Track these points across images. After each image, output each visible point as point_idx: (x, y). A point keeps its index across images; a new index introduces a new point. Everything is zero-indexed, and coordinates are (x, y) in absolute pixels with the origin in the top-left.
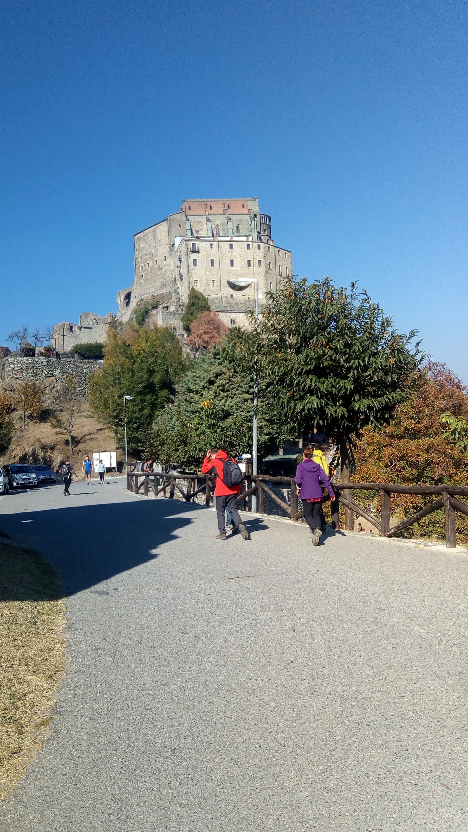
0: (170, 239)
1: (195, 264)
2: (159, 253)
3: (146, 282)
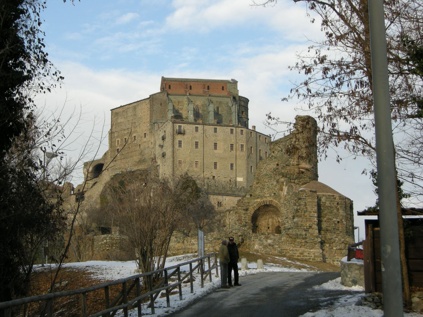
0: (151, 117)
1: (180, 145)
2: (138, 130)
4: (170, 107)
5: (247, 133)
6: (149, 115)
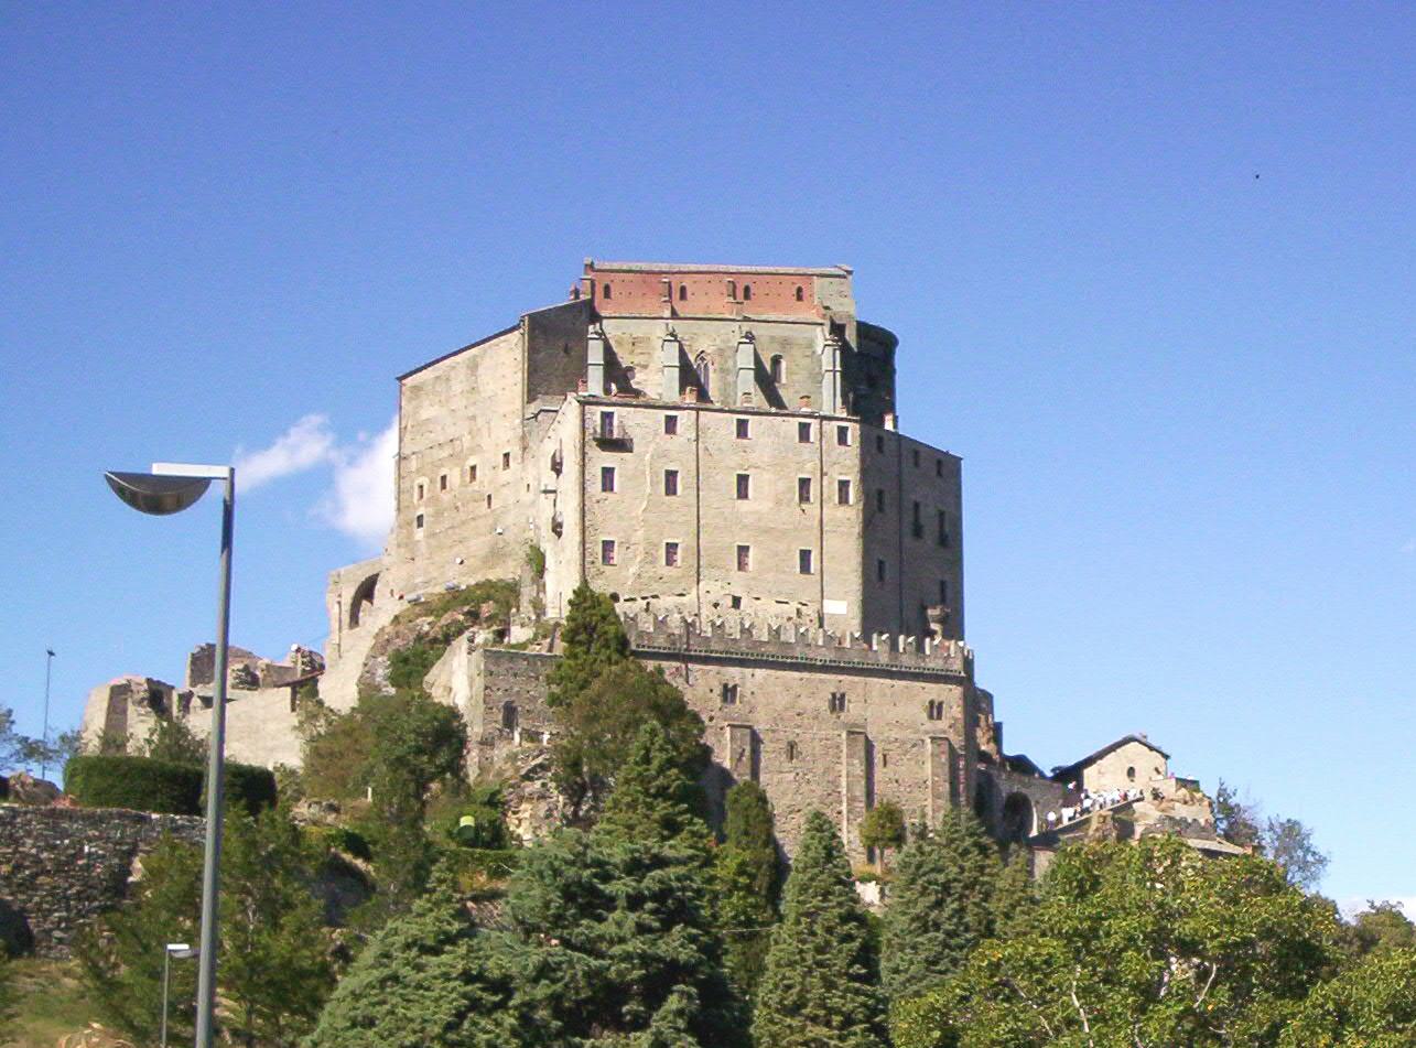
1: (608, 484)
2: (486, 442)
3: (433, 542)
4: (595, 354)
6: (520, 386)
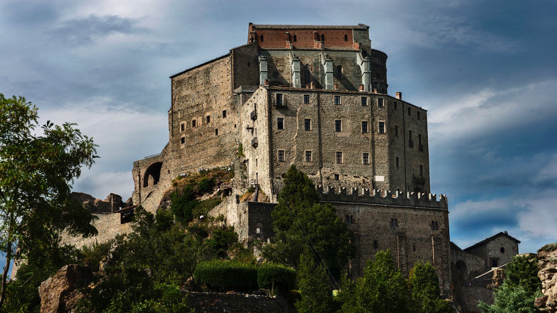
1: (280, 126)
5: (389, 105)
